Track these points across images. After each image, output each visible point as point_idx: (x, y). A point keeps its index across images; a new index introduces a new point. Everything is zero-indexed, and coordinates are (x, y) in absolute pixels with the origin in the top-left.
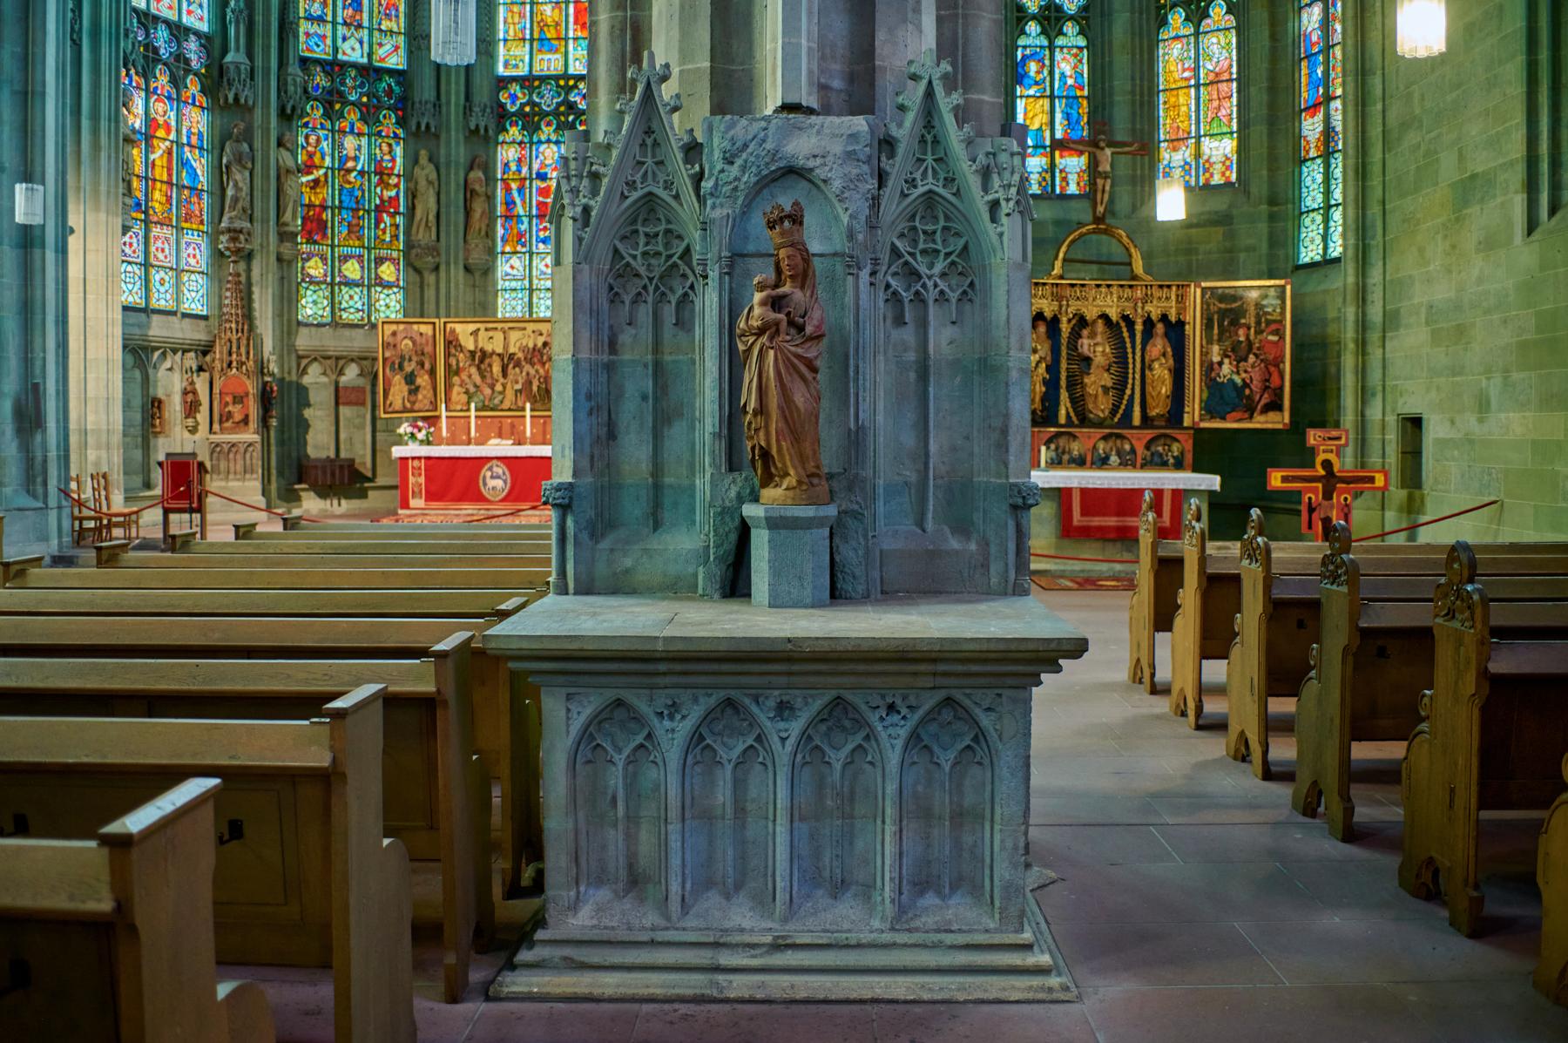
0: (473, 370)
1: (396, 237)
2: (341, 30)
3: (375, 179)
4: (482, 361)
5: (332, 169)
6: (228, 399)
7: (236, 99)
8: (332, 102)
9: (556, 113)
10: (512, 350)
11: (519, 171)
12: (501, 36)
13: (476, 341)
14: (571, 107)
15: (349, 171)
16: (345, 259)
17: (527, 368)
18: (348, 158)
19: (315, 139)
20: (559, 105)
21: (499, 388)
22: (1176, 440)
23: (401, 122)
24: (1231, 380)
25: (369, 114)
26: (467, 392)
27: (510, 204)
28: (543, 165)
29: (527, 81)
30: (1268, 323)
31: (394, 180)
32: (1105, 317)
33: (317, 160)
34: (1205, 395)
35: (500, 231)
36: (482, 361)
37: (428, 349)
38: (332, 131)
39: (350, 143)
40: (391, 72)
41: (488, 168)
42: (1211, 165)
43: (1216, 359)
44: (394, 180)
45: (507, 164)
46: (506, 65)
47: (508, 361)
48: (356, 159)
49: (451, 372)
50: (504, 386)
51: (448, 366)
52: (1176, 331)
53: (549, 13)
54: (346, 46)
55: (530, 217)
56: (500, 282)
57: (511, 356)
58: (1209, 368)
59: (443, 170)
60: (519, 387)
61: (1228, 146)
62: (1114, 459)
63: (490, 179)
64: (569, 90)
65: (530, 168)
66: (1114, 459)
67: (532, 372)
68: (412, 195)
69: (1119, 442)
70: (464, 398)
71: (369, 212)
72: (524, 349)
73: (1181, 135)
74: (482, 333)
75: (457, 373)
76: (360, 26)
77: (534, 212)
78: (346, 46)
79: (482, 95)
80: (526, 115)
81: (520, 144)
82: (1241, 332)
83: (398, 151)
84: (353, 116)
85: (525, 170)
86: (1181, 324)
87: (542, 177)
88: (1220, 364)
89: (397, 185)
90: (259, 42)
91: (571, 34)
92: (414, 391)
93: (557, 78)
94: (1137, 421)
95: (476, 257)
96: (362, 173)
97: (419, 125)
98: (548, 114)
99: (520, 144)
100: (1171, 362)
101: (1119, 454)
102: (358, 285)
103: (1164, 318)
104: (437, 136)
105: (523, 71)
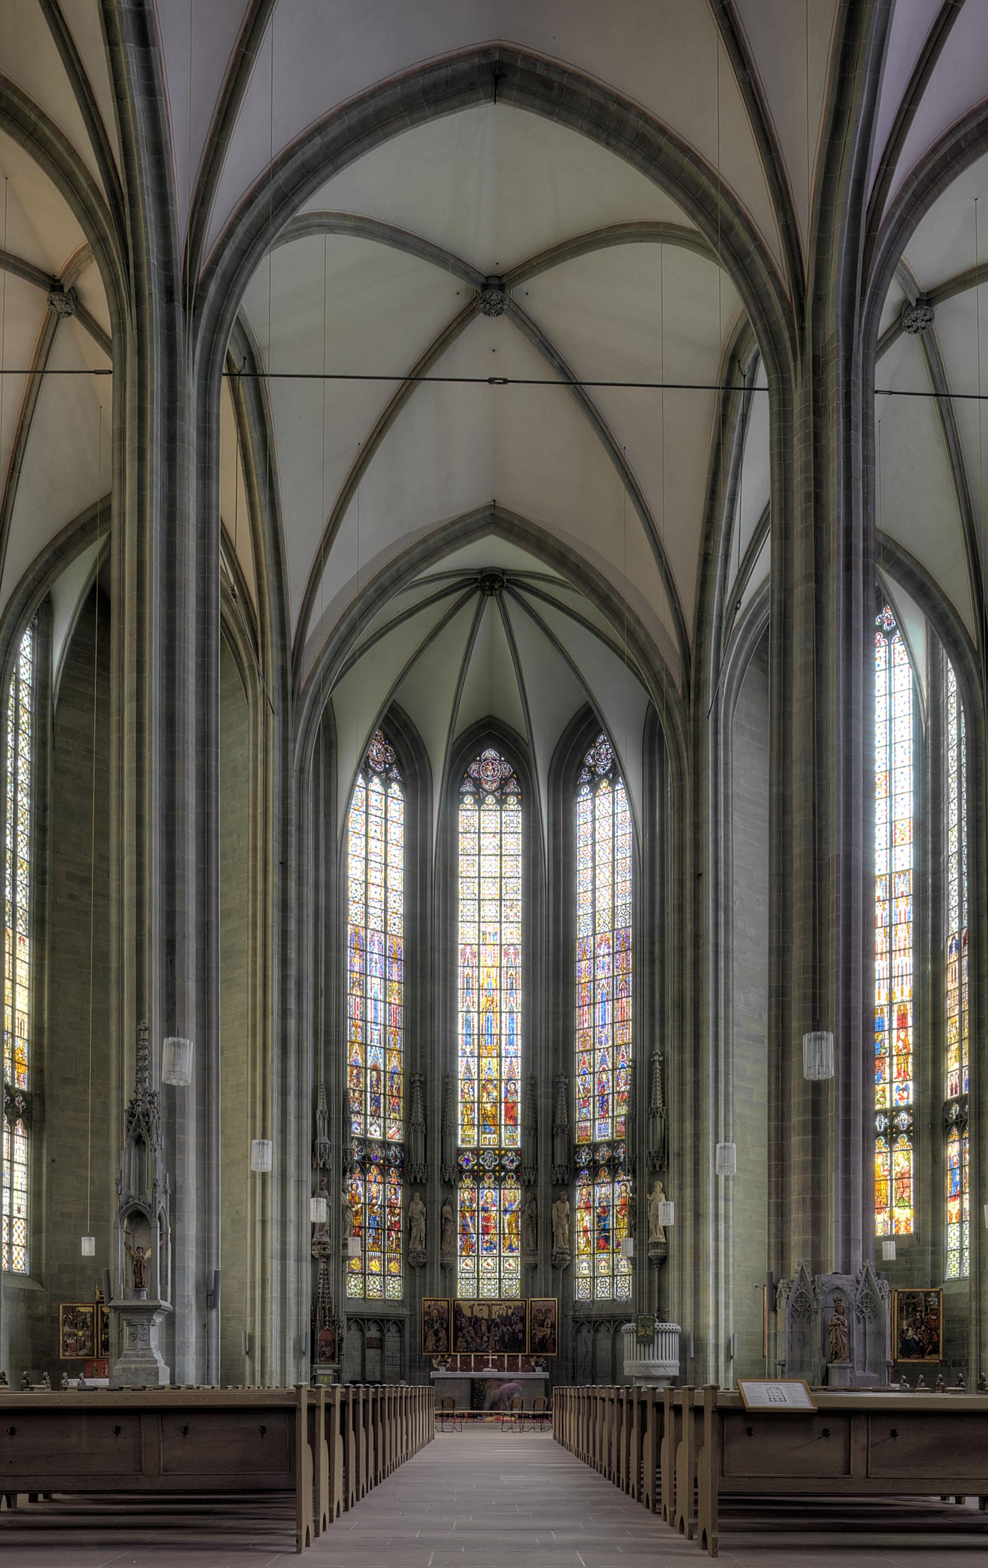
0: (470, 1328)
1: (398, 1245)
2: (369, 1119)
3: (387, 1210)
4: (475, 1323)
5: (365, 1204)
6: (323, 1343)
7: (324, 1164)
8: (365, 1163)
9: (494, 1171)
10: (493, 1317)
11: (471, 1206)
12: (460, 1122)
13: (472, 1311)
14: (503, 1168)
15: (374, 1205)
16: (371, 1259)
17: (502, 1327)
18: (373, 1198)
19: (356, 1185)
20: (495, 1166)
21: (485, 1339)
23: (401, 1176)
25: (384, 1171)
26: (467, 1341)
27: (465, 1226)
28: (486, 1202)
29: (476, 1152)
31: (397, 1211)
33: (357, 1199)
35: (459, 1243)
36: (475, 1323)
37: (445, 1316)
38: (365, 1181)
39: (374, 1188)
40: (396, 1144)
41: (453, 1204)
44: (397, 1211)
45: (463, 1202)
46: (463, 1141)
47: (491, 1324)
48: (377, 1198)
49: (458, 1329)
50: (488, 1338)
51: (455, 1325)
53: (489, 1108)
54: (372, 1129)
55: (478, 1234)
56: (459, 1274)
57: (493, 1321)
59: (428, 1205)
60: (497, 1338)
63: (454, 1211)
64: (501, 1157)
65: (478, 1204)
67: (505, 1330)
68: (409, 1220)
70: (465, 1345)
71: (384, 1230)
72: (499, 1316)
74: (475, 1307)
75: (461, 1329)
76: (379, 1116)
77: (480, 1231)
78: (372, 1129)
79: (451, 1162)
80: (475, 1171)
81: (471, 1189)
83: (400, 1193)
84: (374, 1171)
85: (474, 1205)
87: (485, 1210)
89: (399, 1214)
90: (333, 1129)
91: (503, 1122)
92: (438, 1340)
93: (494, 1150)
95: (447, 1259)
96: (380, 1206)
97: (415, 1179)
98: (489, 1171)
99: (471, 1189)
102: (378, 1275)
104: (424, 1185)
105: (473, 1145)
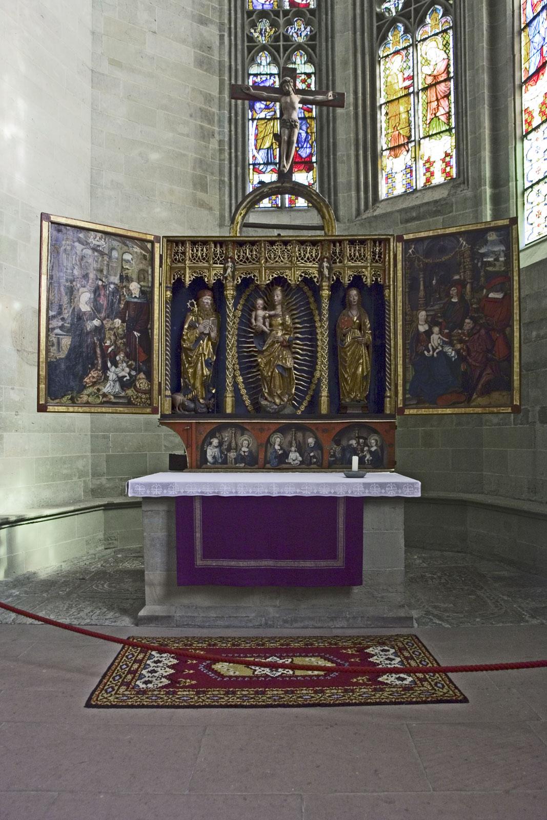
22: (375, 432)
24: (442, 354)
30: (490, 276)
32: (280, 281)
34: (411, 374)
42: (432, 164)
43: (422, 328)
52: (375, 297)
58: (416, 341)
61: (447, 143)
62: (294, 457)
66: (294, 457)
69: (300, 435)
73: (402, 141)
82: (454, 291)
86: (378, 289)
88: (429, 333)
94: (324, 409)
100: (369, 336)
101: (300, 450)
103: (357, 281)
